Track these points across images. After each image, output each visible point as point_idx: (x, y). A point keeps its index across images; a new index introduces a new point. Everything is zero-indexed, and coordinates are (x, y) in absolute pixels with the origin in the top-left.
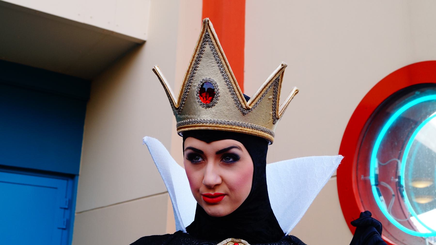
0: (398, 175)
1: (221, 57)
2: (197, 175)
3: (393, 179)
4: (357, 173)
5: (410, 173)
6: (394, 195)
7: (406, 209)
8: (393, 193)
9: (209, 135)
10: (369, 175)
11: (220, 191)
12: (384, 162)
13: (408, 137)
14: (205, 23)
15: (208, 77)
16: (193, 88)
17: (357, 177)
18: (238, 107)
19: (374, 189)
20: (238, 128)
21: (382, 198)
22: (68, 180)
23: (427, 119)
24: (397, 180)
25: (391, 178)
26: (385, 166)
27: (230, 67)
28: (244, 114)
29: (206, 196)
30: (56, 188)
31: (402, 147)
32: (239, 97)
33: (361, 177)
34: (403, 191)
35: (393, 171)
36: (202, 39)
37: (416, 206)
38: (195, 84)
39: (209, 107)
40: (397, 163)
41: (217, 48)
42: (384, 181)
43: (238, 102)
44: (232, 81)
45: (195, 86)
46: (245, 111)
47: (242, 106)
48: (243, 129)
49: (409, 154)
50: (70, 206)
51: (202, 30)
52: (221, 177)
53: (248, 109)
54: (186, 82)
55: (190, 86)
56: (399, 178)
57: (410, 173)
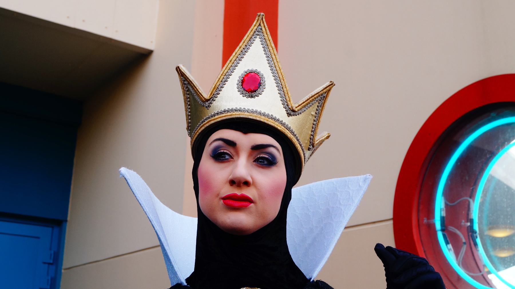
0: (470, 218)
3: (463, 223)
4: (418, 216)
5: (485, 215)
6: (465, 243)
7: (480, 259)
8: (464, 240)
10: (433, 217)
12: (452, 201)
13: (482, 170)
17: (418, 220)
19: (440, 236)
21: (450, 246)
22: (53, 227)
23: (506, 147)
25: (461, 222)
30: (38, 238)
31: (475, 183)
33: (423, 220)
34: (477, 237)
35: (464, 212)
40: (469, 202)
42: (452, 225)
49: (483, 191)
50: (56, 260)
56: (471, 221)
57: (485, 215)
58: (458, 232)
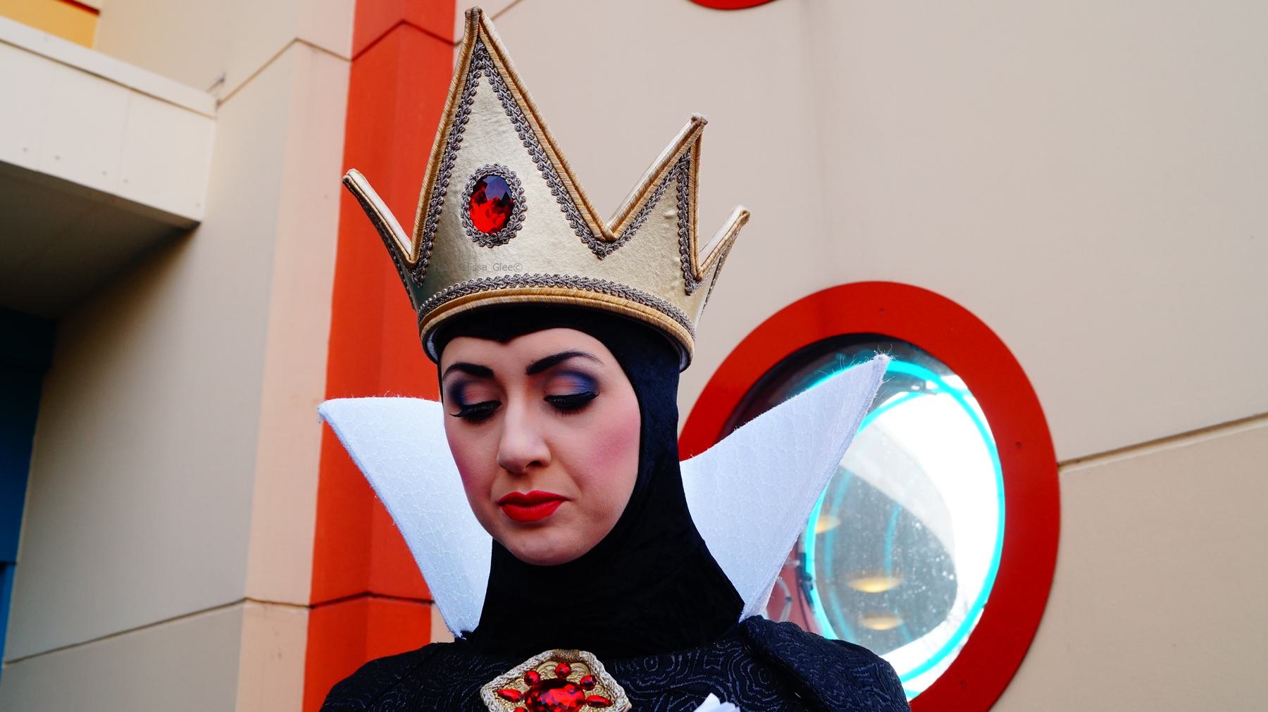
2: (480, 444)
15: (492, 164)
16: (453, 199)
18: (579, 234)
20: (584, 292)
28: (600, 255)
29: (510, 500)
38: (458, 188)
39: (499, 242)
43: (581, 222)
45: (456, 192)
46: (603, 245)
47: (591, 234)
48: (600, 295)
53: (610, 240)
55: (444, 195)
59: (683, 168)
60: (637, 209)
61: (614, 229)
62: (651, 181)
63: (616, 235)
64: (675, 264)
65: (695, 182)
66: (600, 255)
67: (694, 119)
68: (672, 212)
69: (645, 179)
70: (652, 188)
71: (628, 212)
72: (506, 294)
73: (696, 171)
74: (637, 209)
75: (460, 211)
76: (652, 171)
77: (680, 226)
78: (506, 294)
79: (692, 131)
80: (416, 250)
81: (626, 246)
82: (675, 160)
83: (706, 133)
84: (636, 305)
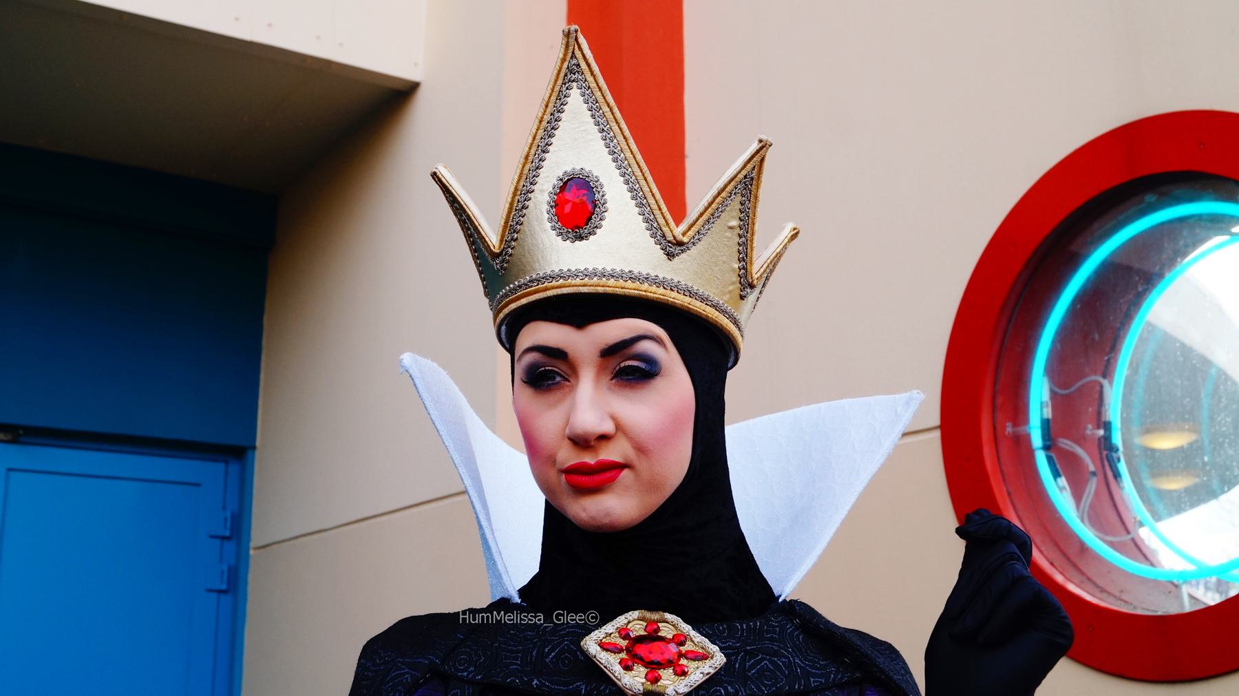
1: (609, 115)
3: (1089, 430)
4: (993, 418)
5: (1135, 415)
6: (1094, 474)
7: (1127, 508)
8: (1092, 468)
9: (583, 308)
10: (1026, 421)
11: (611, 453)
12: (1064, 386)
13: (1128, 318)
14: (567, 35)
15: (578, 168)
17: (995, 429)
18: (653, 236)
19: (1041, 459)
20: (654, 288)
21: (1063, 481)
22: (227, 462)
24: (1101, 432)
25: (1085, 428)
26: (1068, 396)
27: (631, 141)
28: (671, 256)
30: (198, 485)
31: (1112, 345)
32: (657, 212)
33: (1004, 427)
34: (1119, 460)
36: (562, 75)
37: (1154, 498)
38: (545, 187)
39: (581, 238)
40: (1101, 387)
41: (598, 94)
42: (1067, 438)
44: (638, 173)
45: (542, 191)
46: (673, 248)
47: (664, 236)
48: (668, 292)
49: (1131, 364)
50: (236, 529)
51: (561, 56)
52: (614, 419)
53: (680, 244)
54: (522, 183)
56: (1107, 426)
57: (1135, 415)
58: (1080, 451)
59: (747, 184)
60: (705, 217)
61: (684, 234)
62: (719, 194)
63: (685, 239)
64: (734, 270)
65: (756, 197)
66: (671, 256)
67: (761, 141)
68: (735, 223)
69: (714, 191)
70: (719, 199)
71: (697, 220)
72: (585, 285)
73: (758, 188)
74: (705, 217)
75: (545, 207)
76: (720, 184)
77: (740, 236)
78: (585, 285)
79: (758, 152)
80: (501, 241)
81: (694, 250)
82: (741, 176)
83: (770, 155)
84: (698, 304)
